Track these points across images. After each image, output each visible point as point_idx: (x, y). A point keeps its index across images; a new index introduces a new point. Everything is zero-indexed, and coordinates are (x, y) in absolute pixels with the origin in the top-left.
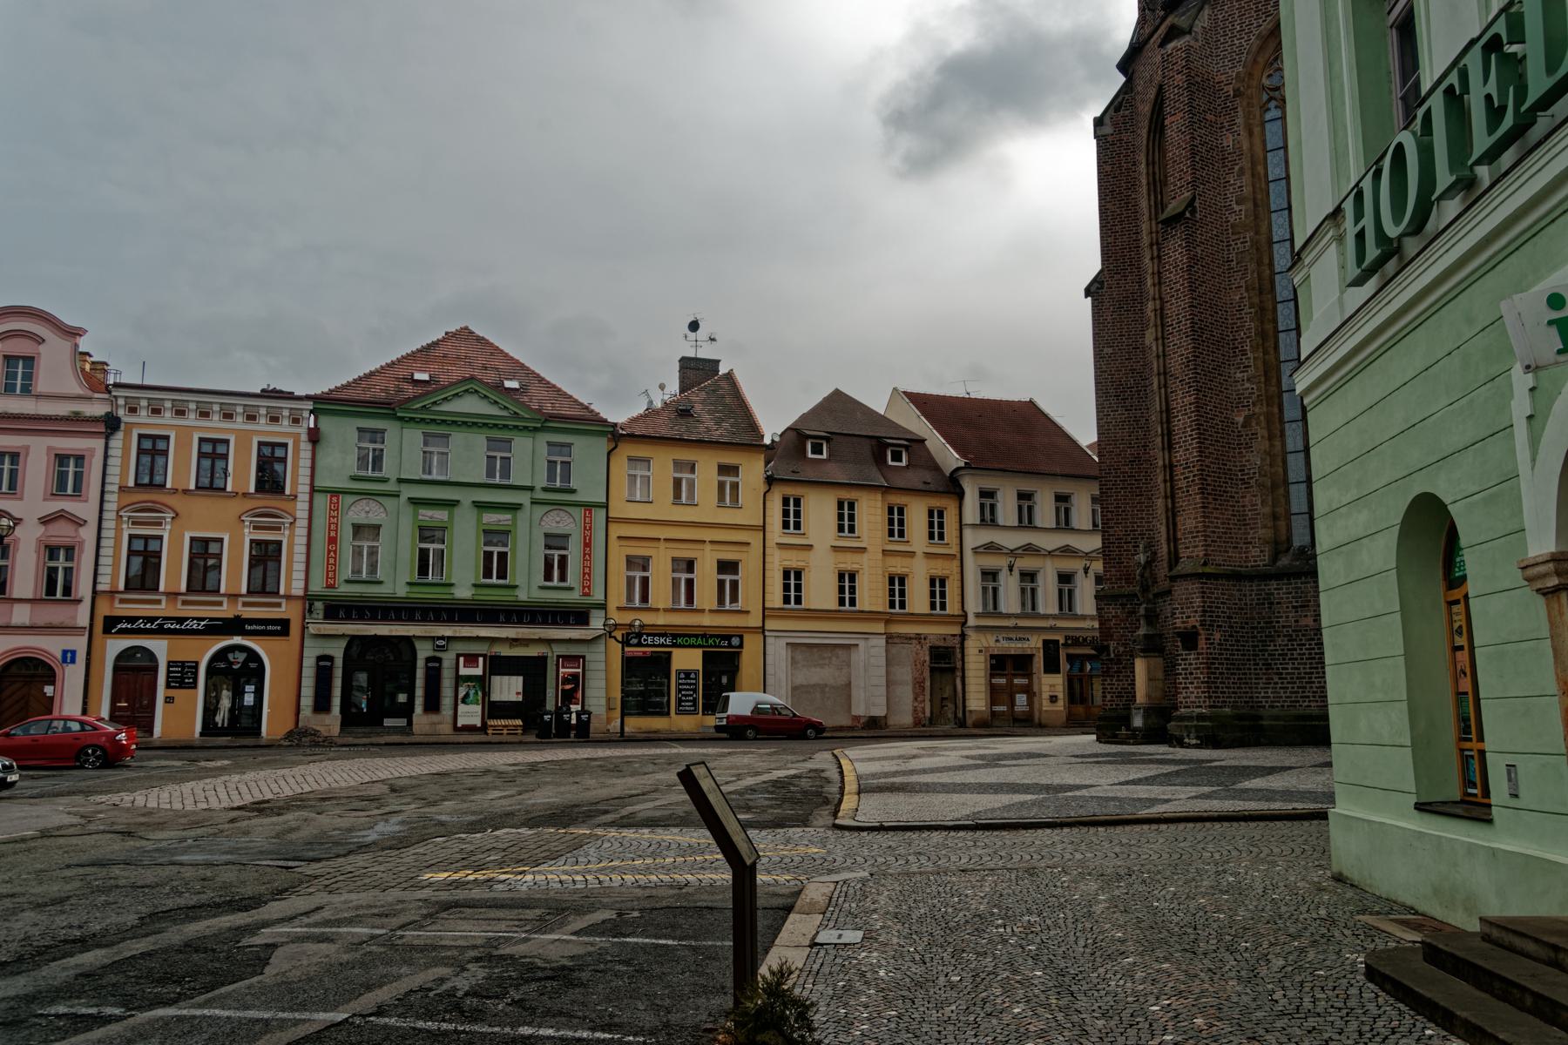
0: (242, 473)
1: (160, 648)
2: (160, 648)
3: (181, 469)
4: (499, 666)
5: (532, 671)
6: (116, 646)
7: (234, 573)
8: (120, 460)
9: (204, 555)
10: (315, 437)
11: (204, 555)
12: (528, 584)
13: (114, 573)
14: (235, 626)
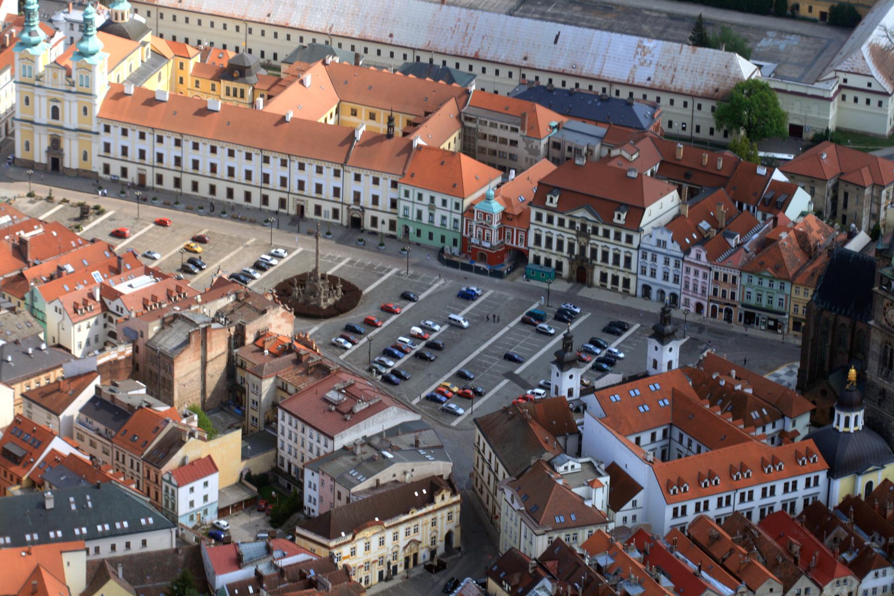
0: (730, 280)
1: (718, 305)
2: (718, 305)
3: (721, 278)
4: (772, 319)
5: (776, 321)
6: (711, 304)
7: (729, 296)
8: (712, 276)
9: (724, 292)
10: (741, 275)
11: (724, 292)
12: (775, 306)
13: (711, 293)
14: (728, 304)
